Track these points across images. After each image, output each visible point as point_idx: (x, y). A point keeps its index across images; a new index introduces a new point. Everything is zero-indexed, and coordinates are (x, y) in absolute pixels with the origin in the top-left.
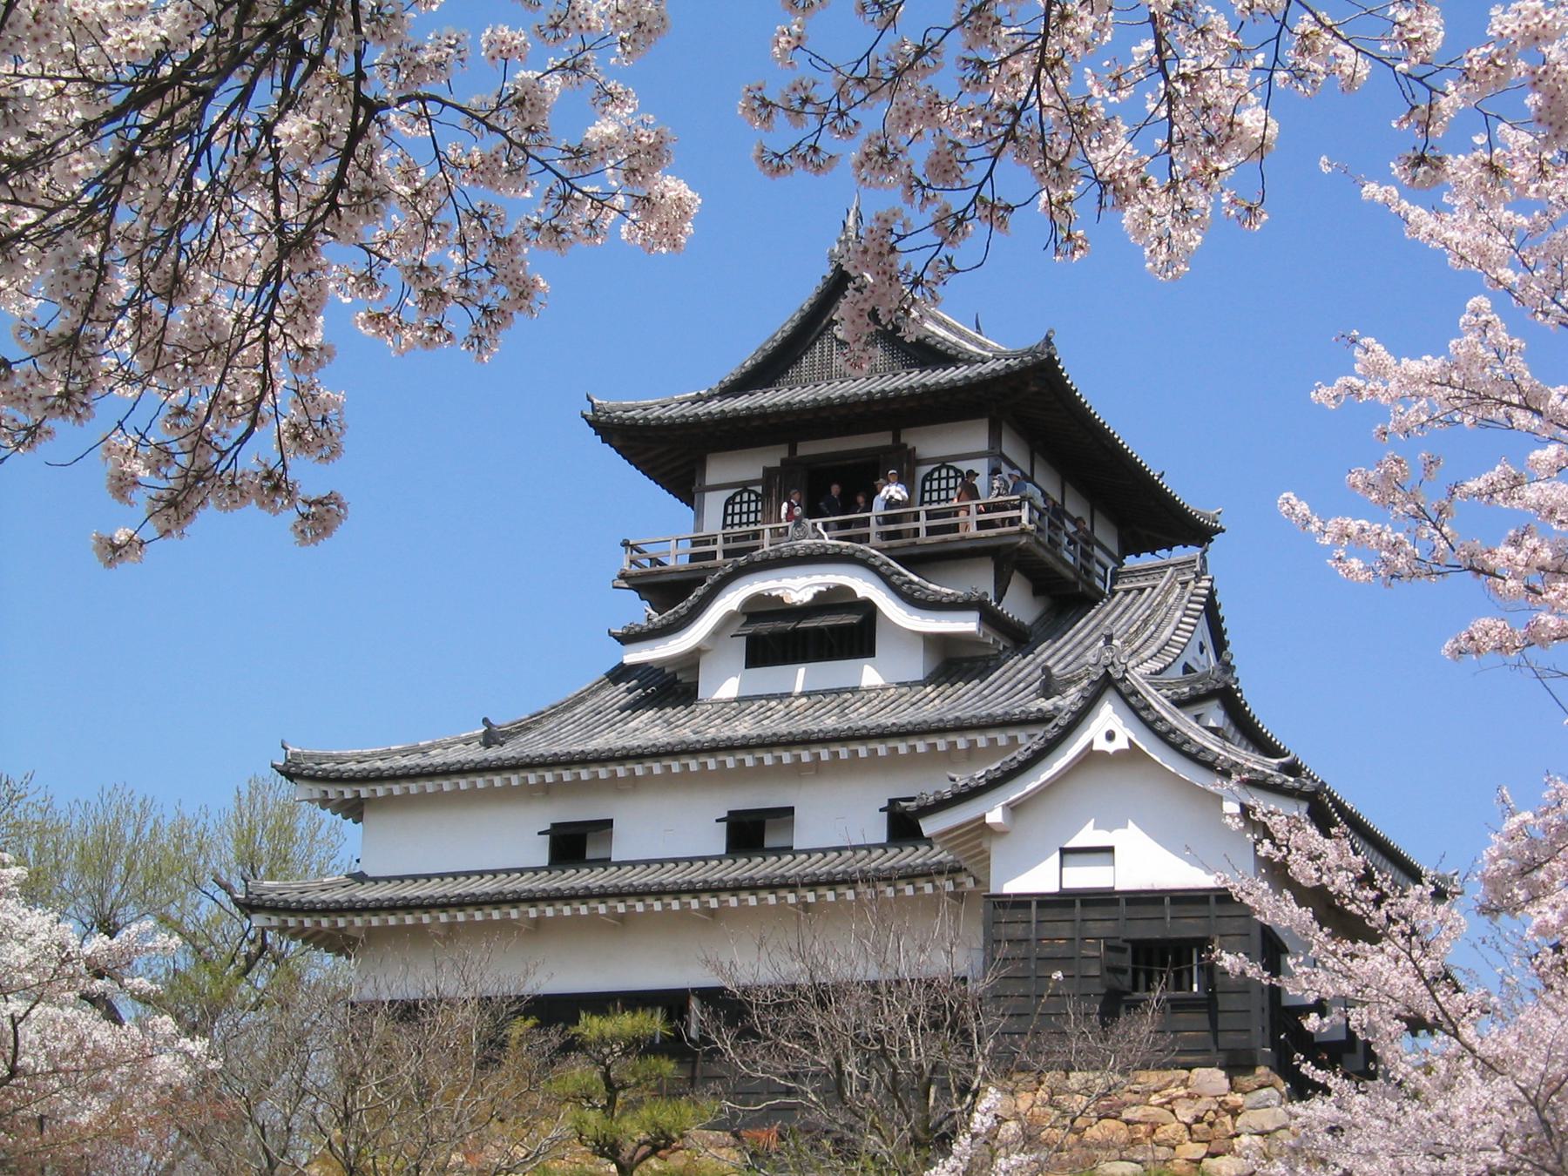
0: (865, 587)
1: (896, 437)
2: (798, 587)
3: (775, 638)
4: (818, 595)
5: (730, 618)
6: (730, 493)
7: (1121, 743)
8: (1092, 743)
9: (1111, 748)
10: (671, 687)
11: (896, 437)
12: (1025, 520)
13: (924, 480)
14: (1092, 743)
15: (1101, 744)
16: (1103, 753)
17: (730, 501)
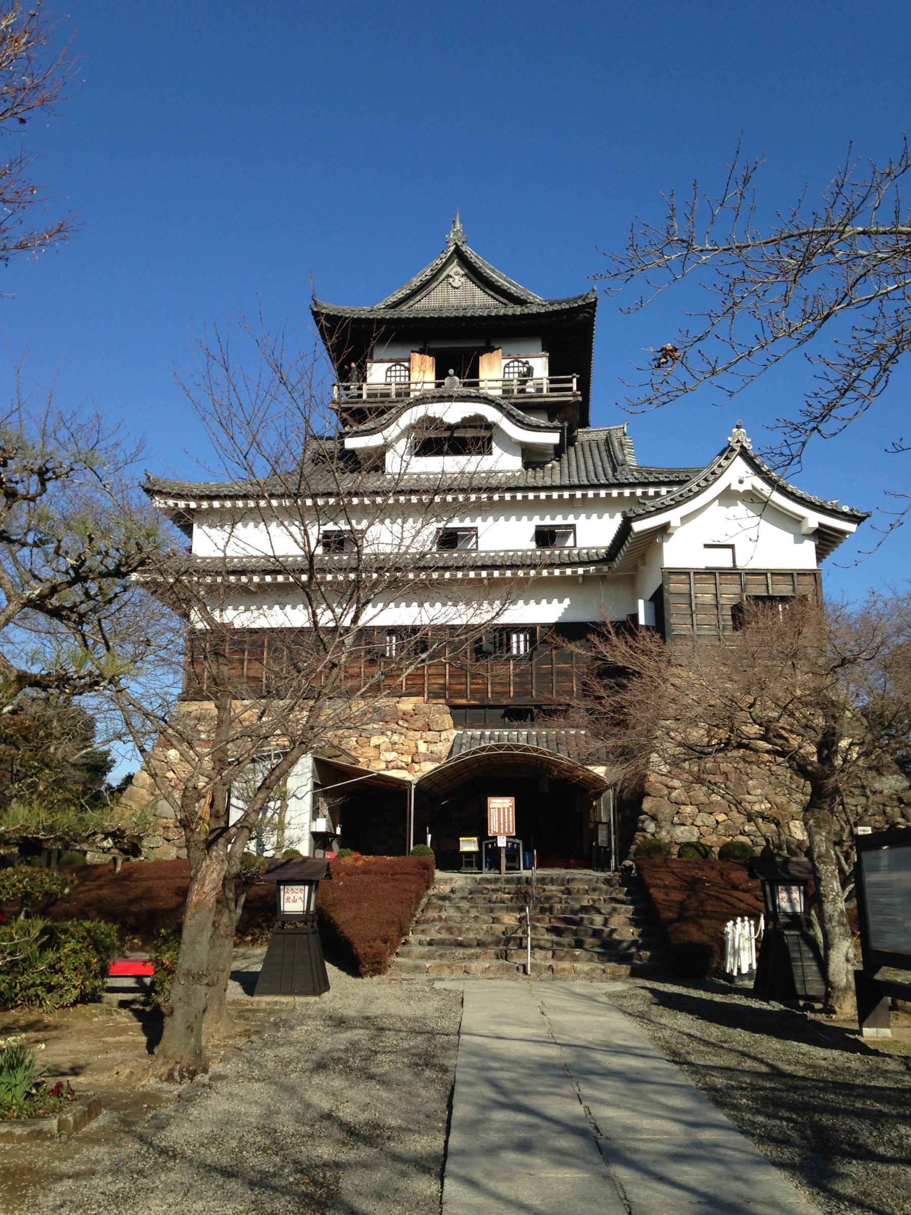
0: (492, 414)
1: (488, 343)
2: (453, 413)
3: (434, 441)
4: (465, 420)
5: (412, 428)
6: (390, 365)
7: (746, 486)
8: (729, 486)
9: (741, 488)
10: (375, 461)
11: (488, 343)
12: (575, 388)
13: (505, 367)
14: (729, 486)
15: (736, 486)
16: (737, 491)
17: (389, 369)
